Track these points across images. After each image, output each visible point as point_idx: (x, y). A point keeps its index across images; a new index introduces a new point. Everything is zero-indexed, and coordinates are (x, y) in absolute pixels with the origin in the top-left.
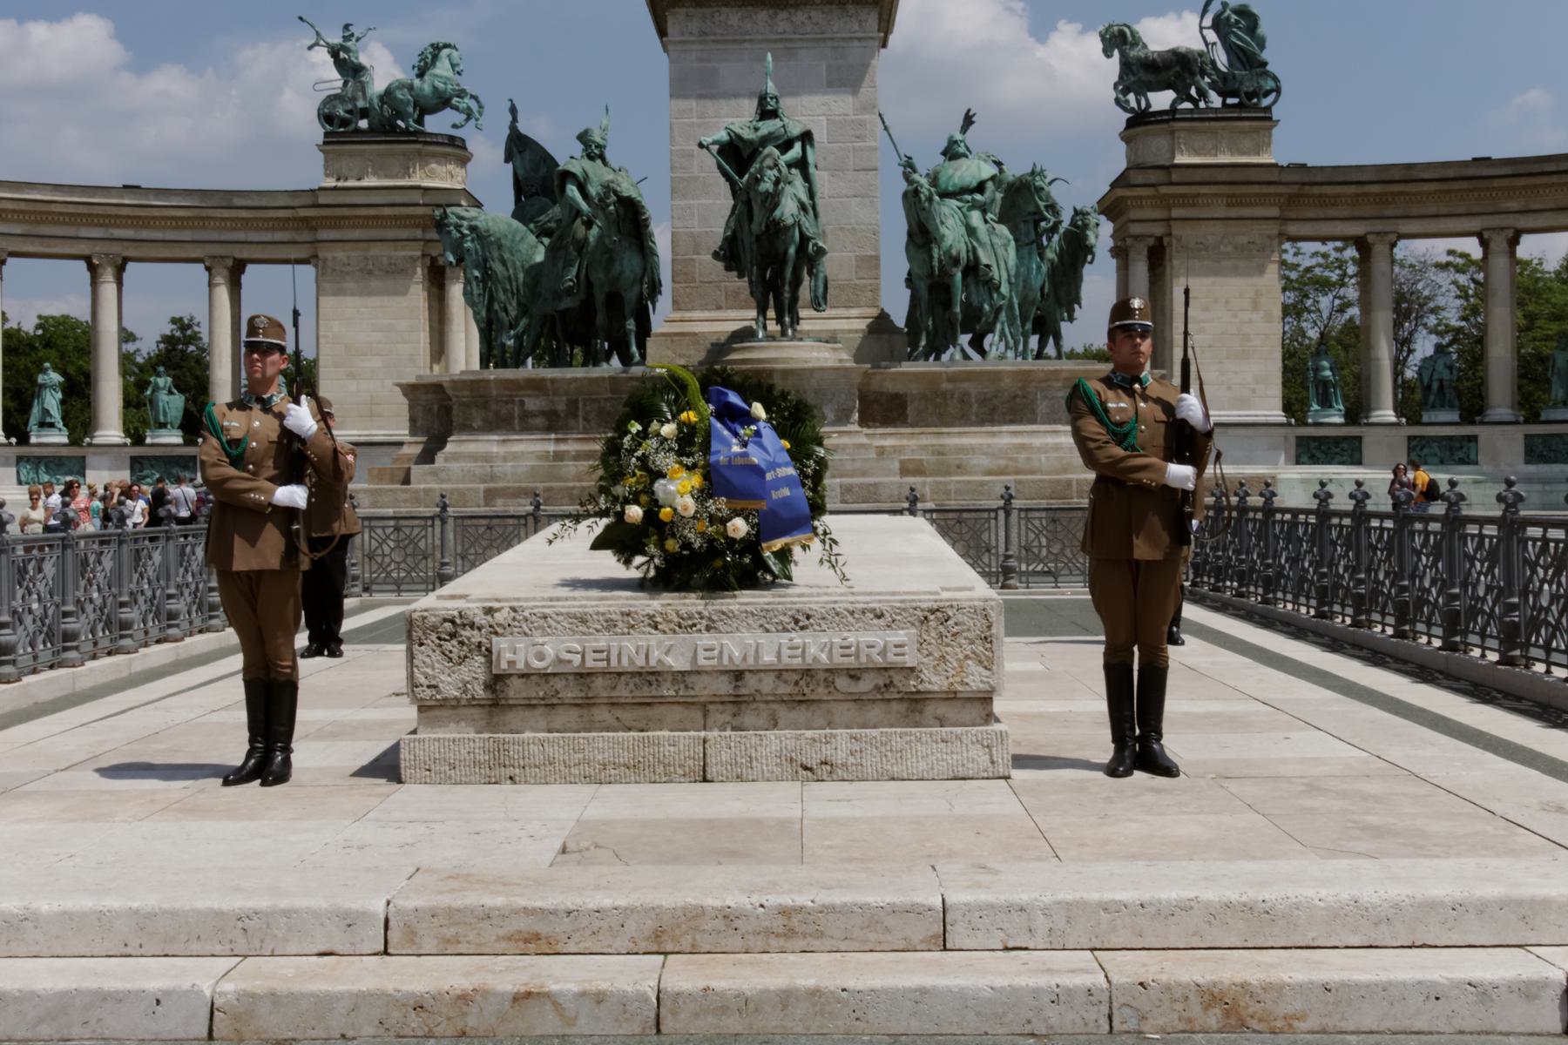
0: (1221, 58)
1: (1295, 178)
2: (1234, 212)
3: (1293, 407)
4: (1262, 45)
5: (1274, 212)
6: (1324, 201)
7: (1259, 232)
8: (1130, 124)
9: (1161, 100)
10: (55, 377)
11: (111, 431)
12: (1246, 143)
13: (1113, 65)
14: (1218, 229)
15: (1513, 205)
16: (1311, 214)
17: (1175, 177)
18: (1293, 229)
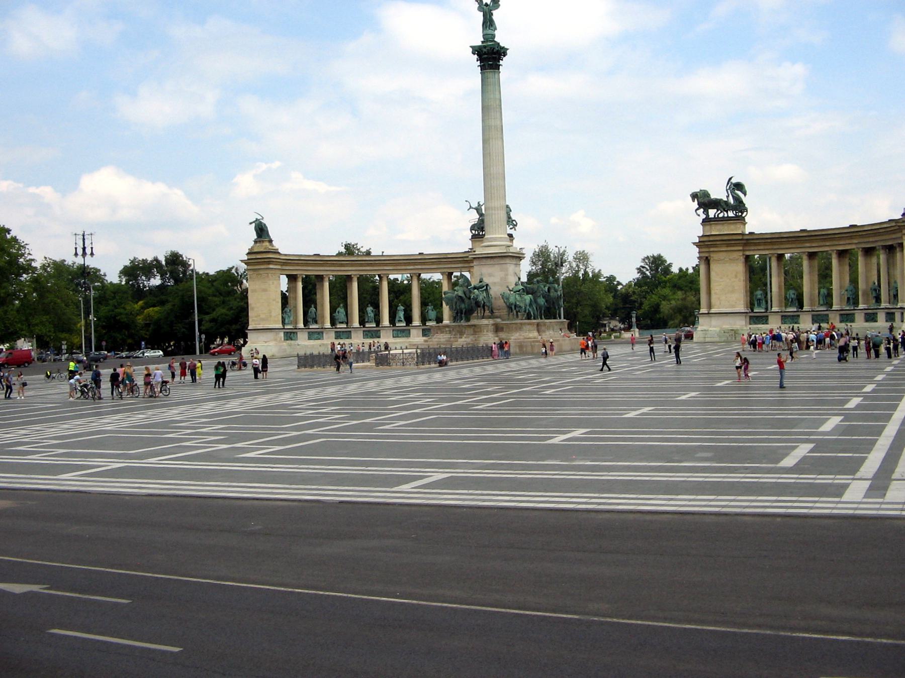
0: (731, 201)
1: (746, 237)
2: (729, 249)
3: (751, 306)
4: (745, 195)
5: (741, 248)
6: (755, 244)
7: (736, 255)
8: (704, 221)
9: (712, 213)
10: (402, 308)
11: (416, 322)
12: (732, 227)
13: (695, 205)
14: (724, 254)
15: (808, 245)
16: (753, 248)
17: (711, 239)
18: (748, 253)
